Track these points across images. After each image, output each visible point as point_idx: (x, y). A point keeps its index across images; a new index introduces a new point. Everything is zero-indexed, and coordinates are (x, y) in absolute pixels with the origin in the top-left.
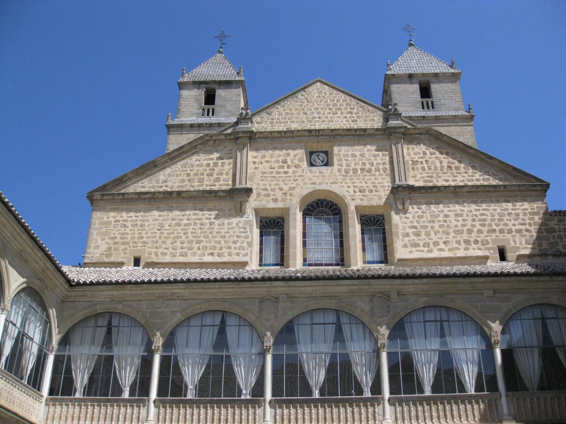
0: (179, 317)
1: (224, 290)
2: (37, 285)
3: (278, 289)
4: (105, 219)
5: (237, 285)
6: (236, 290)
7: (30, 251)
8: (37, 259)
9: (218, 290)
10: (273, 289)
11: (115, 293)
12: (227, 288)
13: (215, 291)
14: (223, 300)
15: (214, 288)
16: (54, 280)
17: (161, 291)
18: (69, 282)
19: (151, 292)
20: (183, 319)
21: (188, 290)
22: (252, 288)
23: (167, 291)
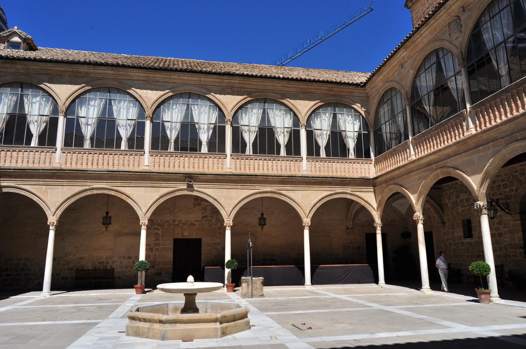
0: (412, 73)
1: (424, 35)
2: (332, 99)
3: (453, 8)
4: (419, 16)
5: (426, 26)
6: (429, 29)
7: (306, 87)
8: (317, 87)
9: (421, 38)
10: (450, 10)
11: (381, 77)
12: (425, 32)
13: (420, 40)
14: (429, 43)
15: (418, 38)
16: (346, 90)
17: (397, 61)
18: (357, 85)
19: (393, 64)
20: (415, 72)
21: (408, 50)
22: (437, 20)
23: (400, 59)
